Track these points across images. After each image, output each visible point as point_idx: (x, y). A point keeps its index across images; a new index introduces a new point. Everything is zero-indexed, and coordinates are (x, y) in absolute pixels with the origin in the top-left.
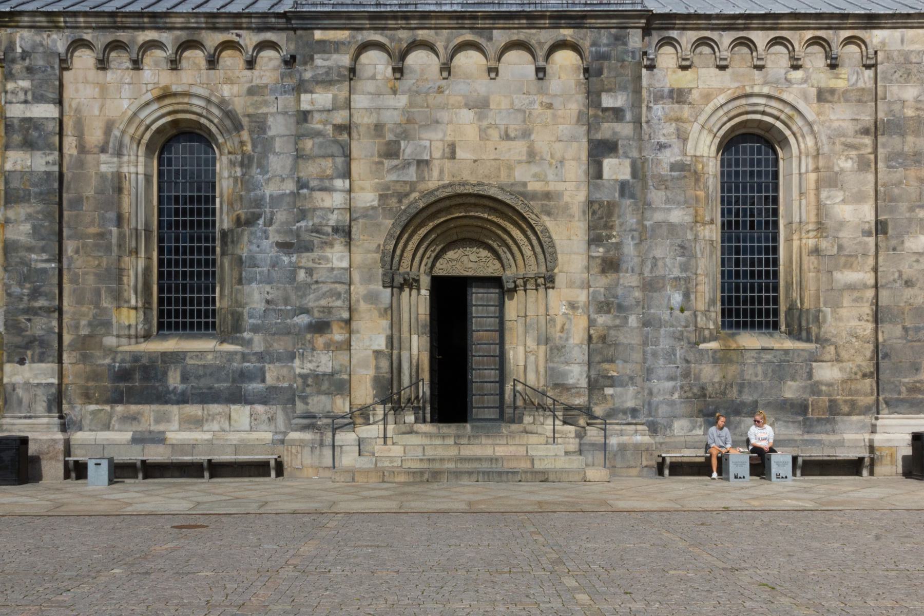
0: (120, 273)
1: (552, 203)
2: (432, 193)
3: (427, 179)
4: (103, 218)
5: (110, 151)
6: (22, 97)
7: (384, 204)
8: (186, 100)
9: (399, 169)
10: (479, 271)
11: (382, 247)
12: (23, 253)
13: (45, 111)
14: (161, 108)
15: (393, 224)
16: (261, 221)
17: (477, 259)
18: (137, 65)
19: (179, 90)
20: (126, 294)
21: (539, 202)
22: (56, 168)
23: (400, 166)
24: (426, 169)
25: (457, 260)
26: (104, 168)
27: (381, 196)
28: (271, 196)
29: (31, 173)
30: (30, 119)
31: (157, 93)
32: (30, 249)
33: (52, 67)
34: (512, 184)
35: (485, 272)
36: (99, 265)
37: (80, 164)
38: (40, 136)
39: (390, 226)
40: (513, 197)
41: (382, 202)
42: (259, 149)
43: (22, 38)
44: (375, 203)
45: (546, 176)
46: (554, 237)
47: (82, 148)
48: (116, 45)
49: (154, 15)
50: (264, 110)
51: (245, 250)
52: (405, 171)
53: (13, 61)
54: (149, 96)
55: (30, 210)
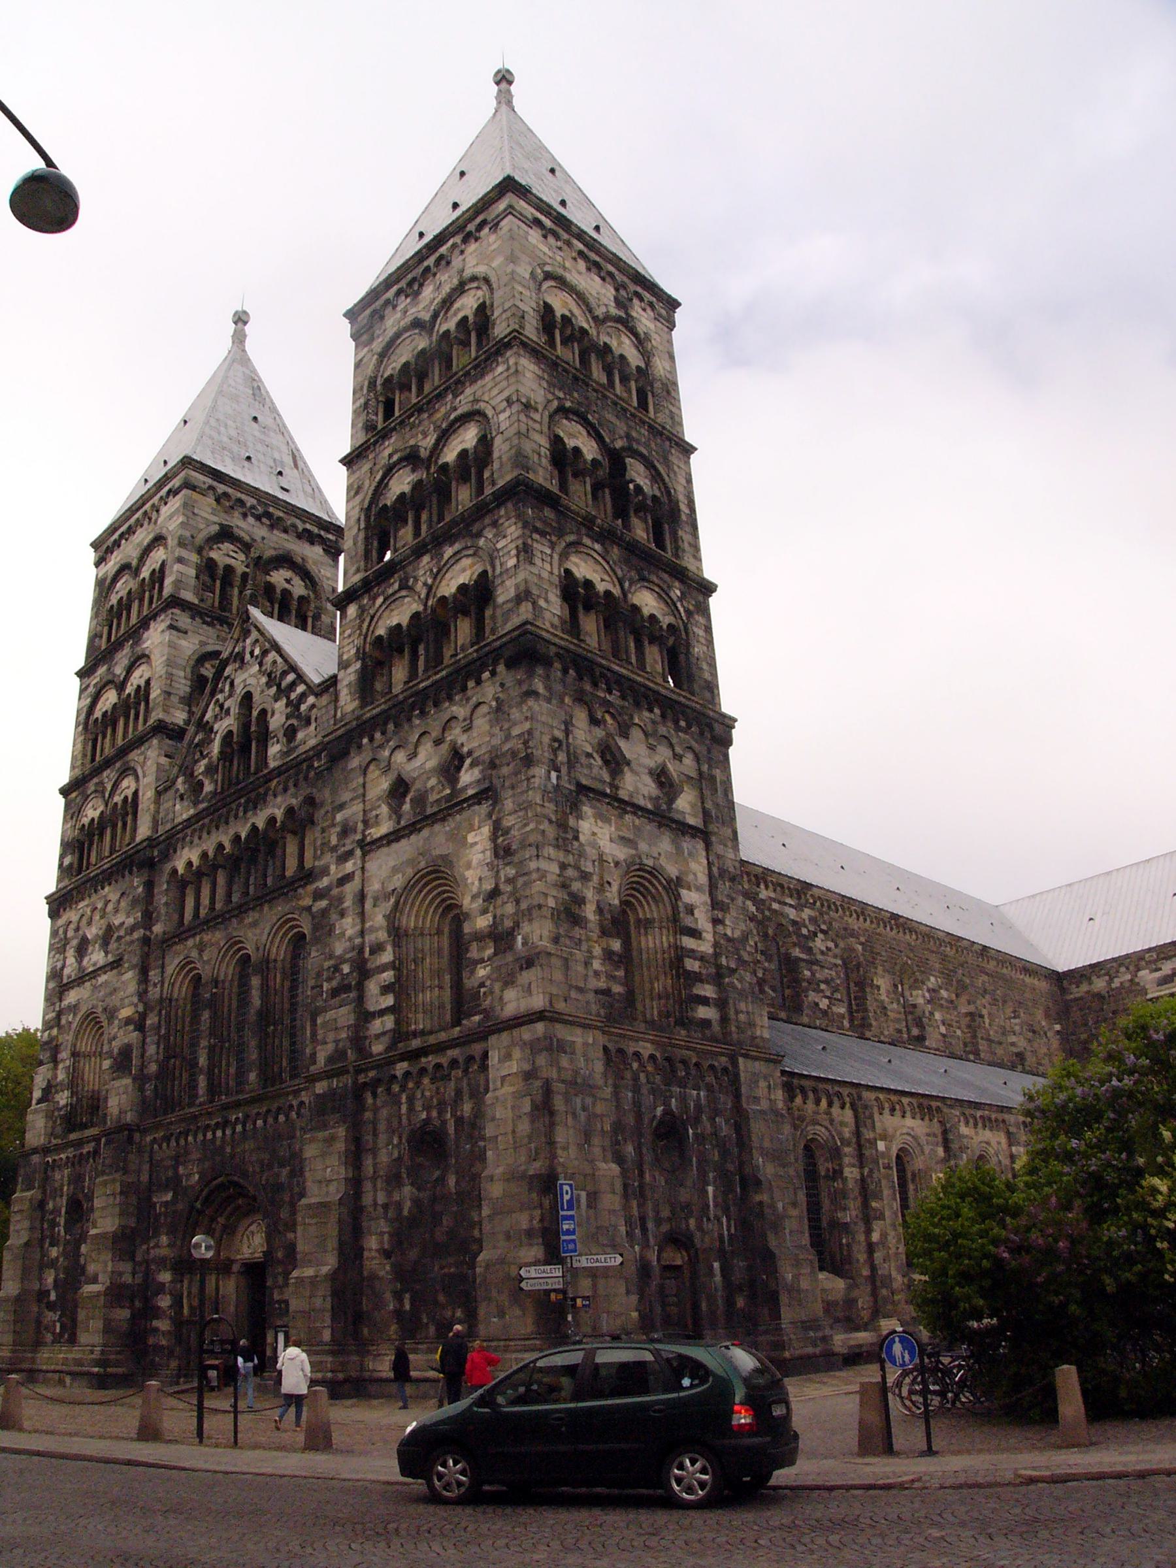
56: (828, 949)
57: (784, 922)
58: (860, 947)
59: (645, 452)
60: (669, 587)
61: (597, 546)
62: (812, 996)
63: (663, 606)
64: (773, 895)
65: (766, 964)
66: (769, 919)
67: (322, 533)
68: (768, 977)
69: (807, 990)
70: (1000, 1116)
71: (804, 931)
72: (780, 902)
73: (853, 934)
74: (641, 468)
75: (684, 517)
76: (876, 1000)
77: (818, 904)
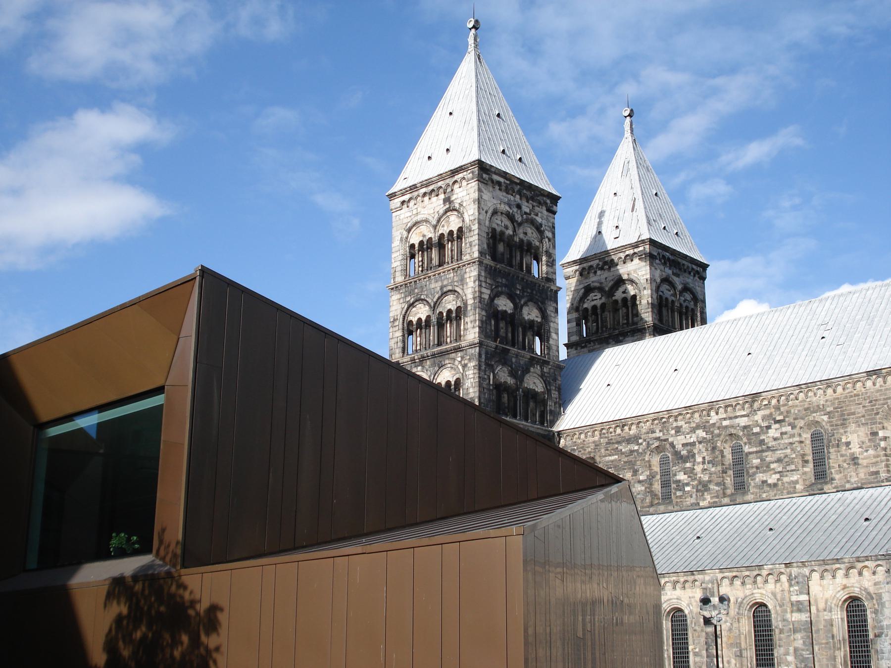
0: (834, 658)
4: (826, 636)
5: (827, 610)
6: (796, 592)
8: (853, 589)
12: (801, 652)
13: (804, 598)
14: (844, 592)
16: (883, 635)
18: (834, 577)
19: (850, 586)
20: (838, 666)
22: (809, 619)
26: (826, 617)
28: (886, 625)
29: (801, 621)
30: (799, 601)
31: (842, 587)
32: (803, 650)
33: (805, 581)
36: (827, 655)
37: (818, 616)
38: (803, 607)
42: (880, 606)
43: (794, 571)
47: (818, 610)
48: (826, 570)
49: (837, 559)
50: (881, 591)
51: (879, 647)
53: (792, 580)
54: (839, 589)
55: (802, 635)
56: (782, 434)
57: (733, 431)
58: (825, 418)
59: (450, 288)
60: (454, 359)
61: (419, 368)
62: (760, 477)
63: (453, 372)
64: (724, 416)
65: (713, 469)
66: (719, 435)
67: (636, 250)
68: (714, 477)
69: (754, 474)
70: (690, 578)
71: (756, 430)
72: (730, 418)
73: (818, 409)
74: (450, 297)
75: (469, 308)
76: (842, 456)
77: (774, 402)
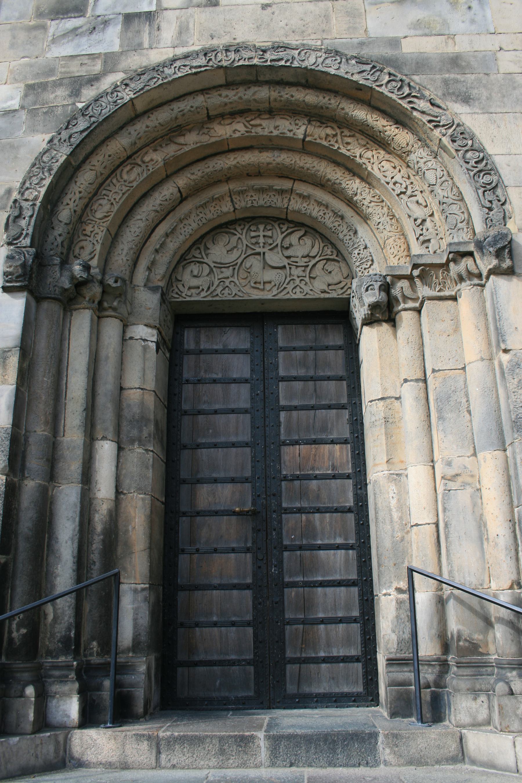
1: (470, 77)
2: (157, 68)
3: (146, 45)
7: (35, 103)
9: (82, 34)
10: (292, 286)
11: (15, 195)
15: (51, 141)
17: (285, 262)
21: (438, 76)
23: (84, 29)
24: (147, 28)
25: (233, 265)
27: (30, 88)
34: (362, 44)
35: (306, 289)
39: (44, 145)
40: (368, 67)
41: (31, 98)
44: (15, 104)
45: (445, 23)
46: (490, 149)
52: (94, 36)
